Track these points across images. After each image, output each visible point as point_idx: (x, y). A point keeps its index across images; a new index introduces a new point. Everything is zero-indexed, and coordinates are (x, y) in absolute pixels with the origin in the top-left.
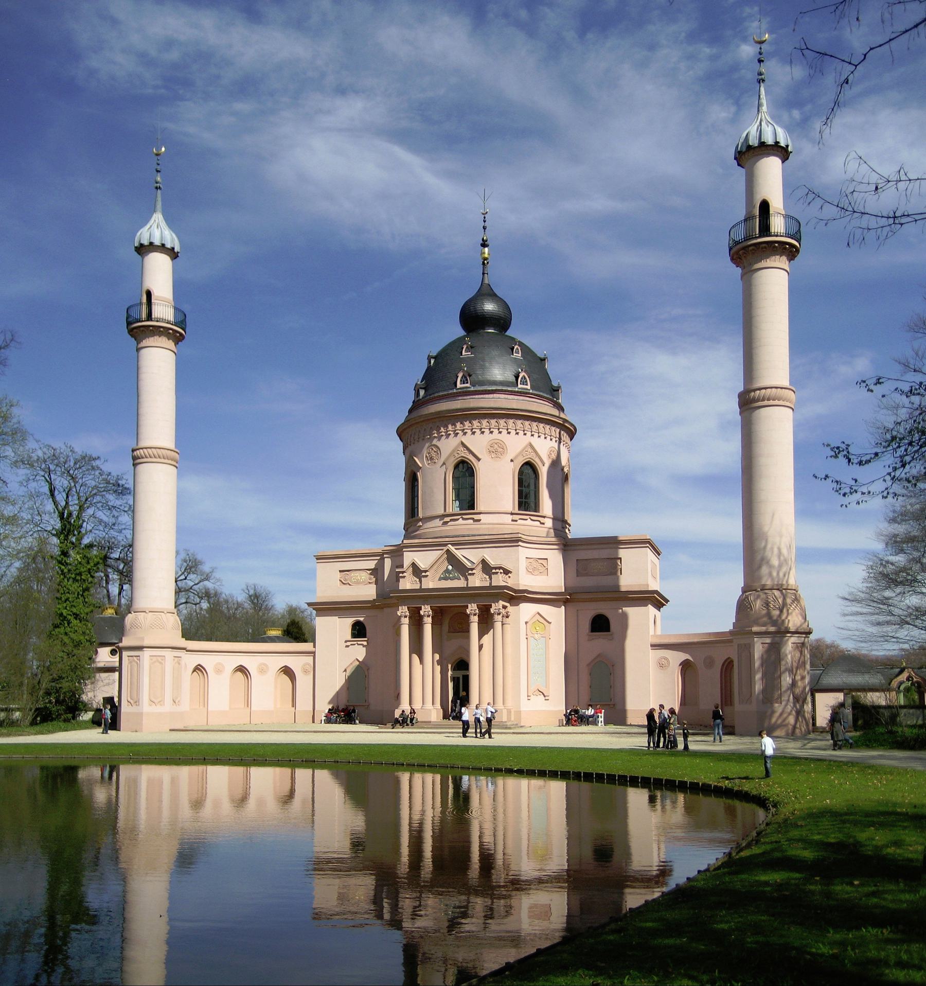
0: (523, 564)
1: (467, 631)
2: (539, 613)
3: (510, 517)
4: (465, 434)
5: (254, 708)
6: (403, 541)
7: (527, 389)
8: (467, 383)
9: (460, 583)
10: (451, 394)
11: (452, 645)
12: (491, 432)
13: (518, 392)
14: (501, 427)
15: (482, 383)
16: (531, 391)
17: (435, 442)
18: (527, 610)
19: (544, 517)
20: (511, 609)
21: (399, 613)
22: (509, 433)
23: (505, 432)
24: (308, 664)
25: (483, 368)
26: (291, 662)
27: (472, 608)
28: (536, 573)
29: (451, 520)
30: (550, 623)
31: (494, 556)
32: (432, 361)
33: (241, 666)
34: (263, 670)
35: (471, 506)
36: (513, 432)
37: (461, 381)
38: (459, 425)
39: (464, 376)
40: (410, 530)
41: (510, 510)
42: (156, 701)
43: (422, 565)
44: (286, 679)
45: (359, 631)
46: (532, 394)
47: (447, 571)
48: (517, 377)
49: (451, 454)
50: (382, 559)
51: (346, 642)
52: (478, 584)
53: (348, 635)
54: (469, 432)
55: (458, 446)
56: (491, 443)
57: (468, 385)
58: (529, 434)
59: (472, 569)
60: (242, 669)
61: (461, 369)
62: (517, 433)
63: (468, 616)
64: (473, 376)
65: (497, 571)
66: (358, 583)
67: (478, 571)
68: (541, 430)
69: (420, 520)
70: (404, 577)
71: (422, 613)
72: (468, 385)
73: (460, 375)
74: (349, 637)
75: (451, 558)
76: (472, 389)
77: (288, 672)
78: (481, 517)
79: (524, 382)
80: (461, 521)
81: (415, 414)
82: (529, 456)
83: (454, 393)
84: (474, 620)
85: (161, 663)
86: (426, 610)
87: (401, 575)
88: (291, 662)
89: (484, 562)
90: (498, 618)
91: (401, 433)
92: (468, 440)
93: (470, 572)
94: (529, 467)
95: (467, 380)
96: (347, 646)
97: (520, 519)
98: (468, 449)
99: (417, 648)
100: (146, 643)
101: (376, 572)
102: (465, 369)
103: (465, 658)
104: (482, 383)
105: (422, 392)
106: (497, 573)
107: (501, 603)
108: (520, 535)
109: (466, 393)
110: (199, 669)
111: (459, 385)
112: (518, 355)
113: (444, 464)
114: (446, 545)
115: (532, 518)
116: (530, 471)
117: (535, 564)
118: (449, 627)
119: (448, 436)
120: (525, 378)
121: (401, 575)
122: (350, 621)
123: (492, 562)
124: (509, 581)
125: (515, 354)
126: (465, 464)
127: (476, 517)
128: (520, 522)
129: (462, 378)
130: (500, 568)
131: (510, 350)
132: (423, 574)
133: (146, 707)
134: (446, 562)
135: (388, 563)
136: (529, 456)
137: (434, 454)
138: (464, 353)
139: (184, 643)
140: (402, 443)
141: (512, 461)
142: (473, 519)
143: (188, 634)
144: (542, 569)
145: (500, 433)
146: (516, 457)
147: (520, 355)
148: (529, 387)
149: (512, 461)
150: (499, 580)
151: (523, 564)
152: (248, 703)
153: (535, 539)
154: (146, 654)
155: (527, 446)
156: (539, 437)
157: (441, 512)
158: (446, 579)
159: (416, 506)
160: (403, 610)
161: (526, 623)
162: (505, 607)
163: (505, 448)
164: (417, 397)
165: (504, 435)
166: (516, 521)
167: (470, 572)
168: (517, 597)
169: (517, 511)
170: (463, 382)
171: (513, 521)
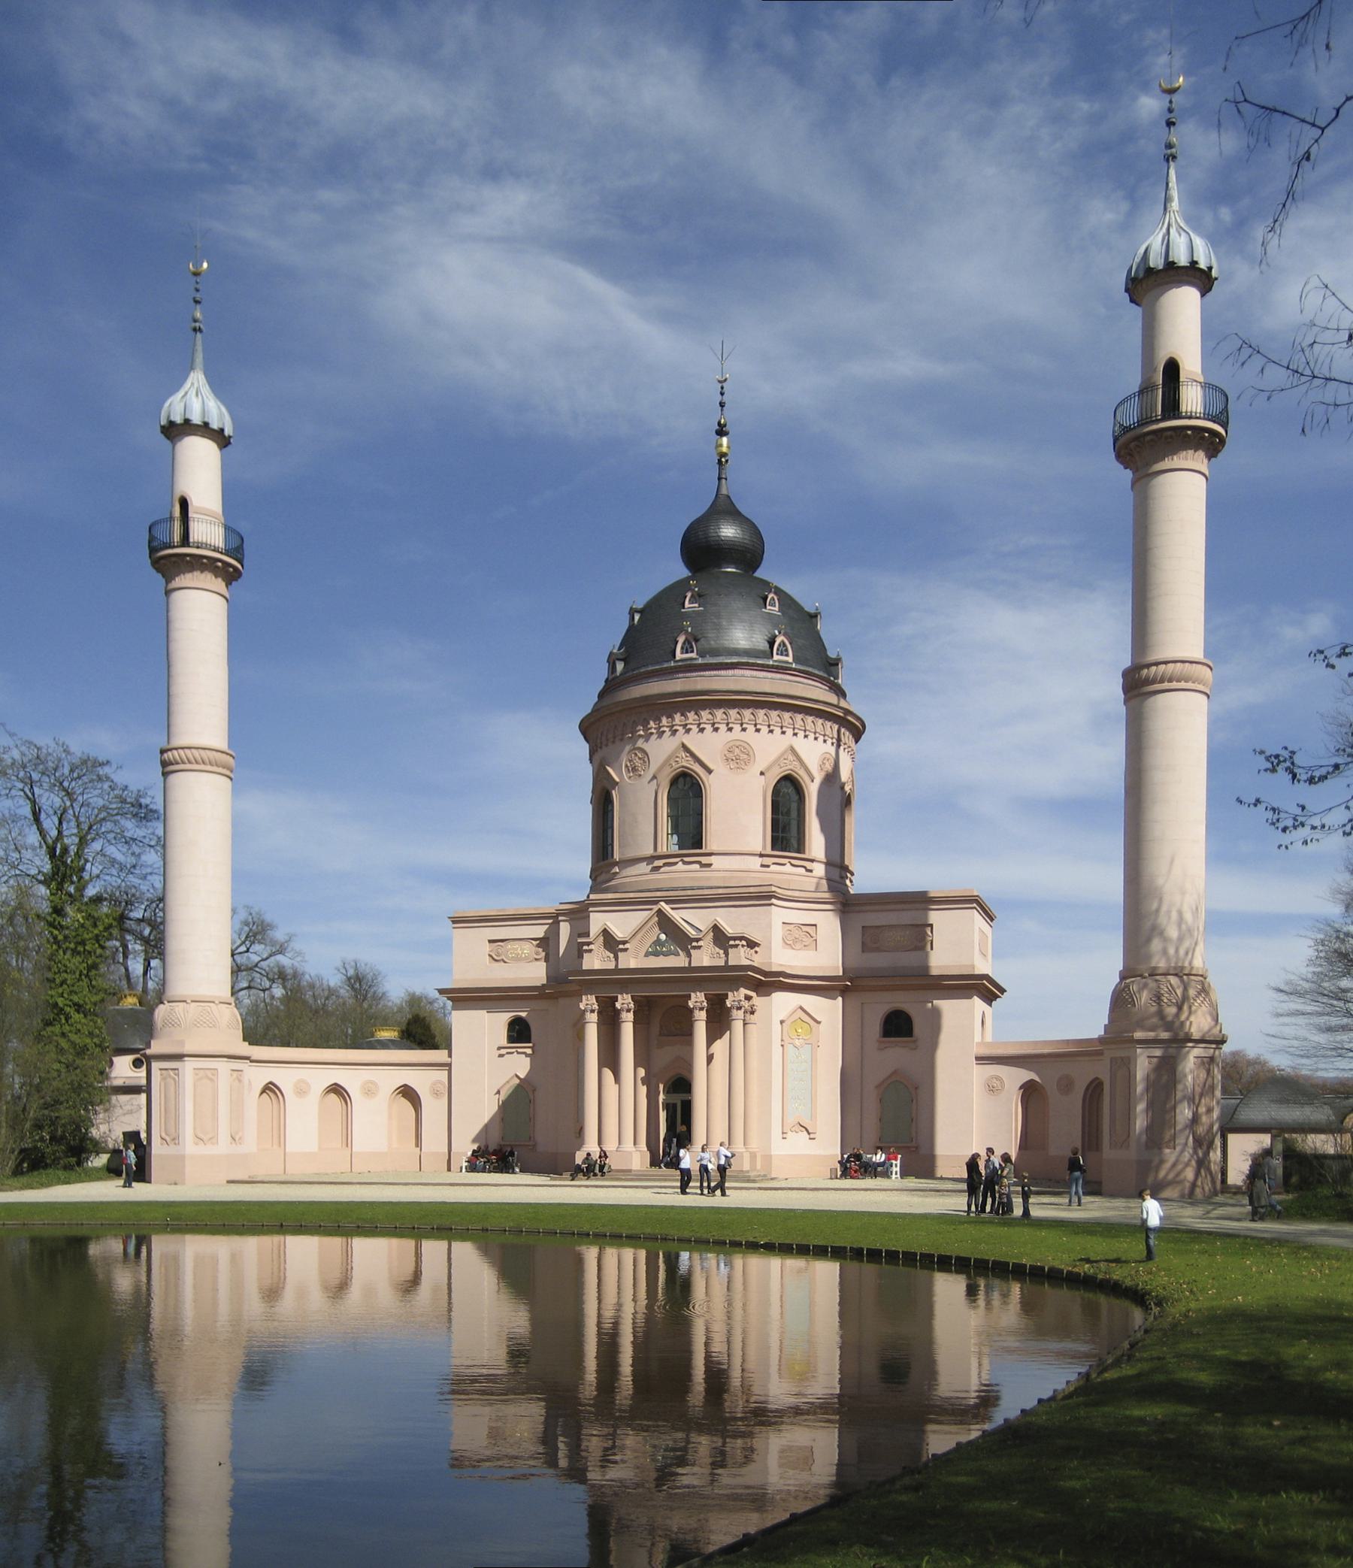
0: (777, 933)
1: (688, 1034)
2: (801, 1008)
3: (759, 861)
4: (688, 731)
6: (588, 897)
7: (787, 662)
8: (692, 652)
9: (679, 961)
10: (666, 669)
11: (664, 1056)
12: (730, 729)
13: (773, 667)
14: (746, 720)
15: (715, 653)
16: (794, 666)
17: (640, 743)
18: (783, 1003)
19: (812, 861)
20: (757, 1001)
21: (582, 1006)
22: (758, 730)
23: (751, 728)
24: (440, 1082)
25: (718, 628)
27: (697, 999)
28: (798, 946)
29: (665, 865)
30: (819, 1023)
31: (731, 920)
32: (637, 617)
33: (335, 1084)
34: (369, 1091)
35: (698, 843)
36: (764, 729)
37: (682, 648)
38: (678, 717)
39: (687, 641)
40: (600, 879)
41: (759, 849)
42: (205, 1139)
43: (619, 934)
44: (406, 1104)
45: (519, 1032)
46: (795, 670)
47: (658, 942)
48: (771, 643)
49: (667, 762)
50: (557, 923)
51: (499, 1048)
52: (706, 962)
53: (502, 1039)
54: (695, 728)
55: (676, 751)
56: (731, 744)
58: (790, 732)
59: (698, 940)
60: (336, 1089)
61: (682, 630)
62: (771, 731)
63: (691, 1011)
64: (702, 642)
65: (737, 942)
66: (518, 959)
67: (707, 943)
68: (810, 726)
69: (616, 864)
70: (590, 951)
71: (618, 1005)
72: (693, 655)
73: (681, 639)
74: (504, 1042)
75: (665, 923)
76: (700, 661)
77: (408, 1093)
79: (783, 651)
80: (680, 866)
81: (608, 701)
82: (790, 766)
83: (671, 668)
85: (211, 1080)
86: (624, 1001)
87: (585, 948)
89: (716, 929)
90: (738, 1015)
91: (587, 728)
92: (693, 740)
93: (694, 944)
94: (789, 784)
95: (692, 647)
96: (501, 1056)
97: (774, 864)
99: (610, 1058)
101: (546, 943)
102: (690, 629)
104: (715, 653)
105: (620, 666)
106: (736, 946)
107: (743, 991)
108: (774, 889)
109: (689, 668)
110: (270, 1089)
111: (679, 655)
112: (774, 609)
113: (654, 777)
114: (656, 903)
115: (793, 862)
116: (791, 790)
117: (797, 933)
118: (661, 1027)
119: (661, 734)
120: (784, 645)
121: (585, 948)
122: (503, 1018)
123: (729, 930)
124: (756, 958)
125: (768, 607)
126: (688, 779)
127: (704, 860)
128: (773, 868)
129: (684, 643)
130: (741, 938)
131: (762, 601)
132: (621, 946)
133: (190, 1146)
134: (657, 929)
135: (565, 929)
136: (790, 767)
137: (638, 763)
138: (687, 604)
139: (245, 1049)
140: (587, 746)
141: (762, 773)
142: (699, 863)
143: (254, 1035)
144: (808, 940)
145: (744, 730)
146: (769, 768)
147: (777, 609)
148: (790, 659)
149: (762, 773)
150: (740, 956)
151: (777, 933)
152: (347, 1140)
153: (797, 894)
154: (189, 1066)
155: (785, 752)
156: (806, 736)
157: (649, 851)
158: (656, 954)
159: (610, 842)
160: (589, 1002)
161: (782, 1022)
162: (748, 998)
163: (751, 753)
164: (612, 673)
166: (768, 866)
167: (694, 944)
168: (768, 983)
169: (769, 851)
170: (685, 651)
171: (762, 866)
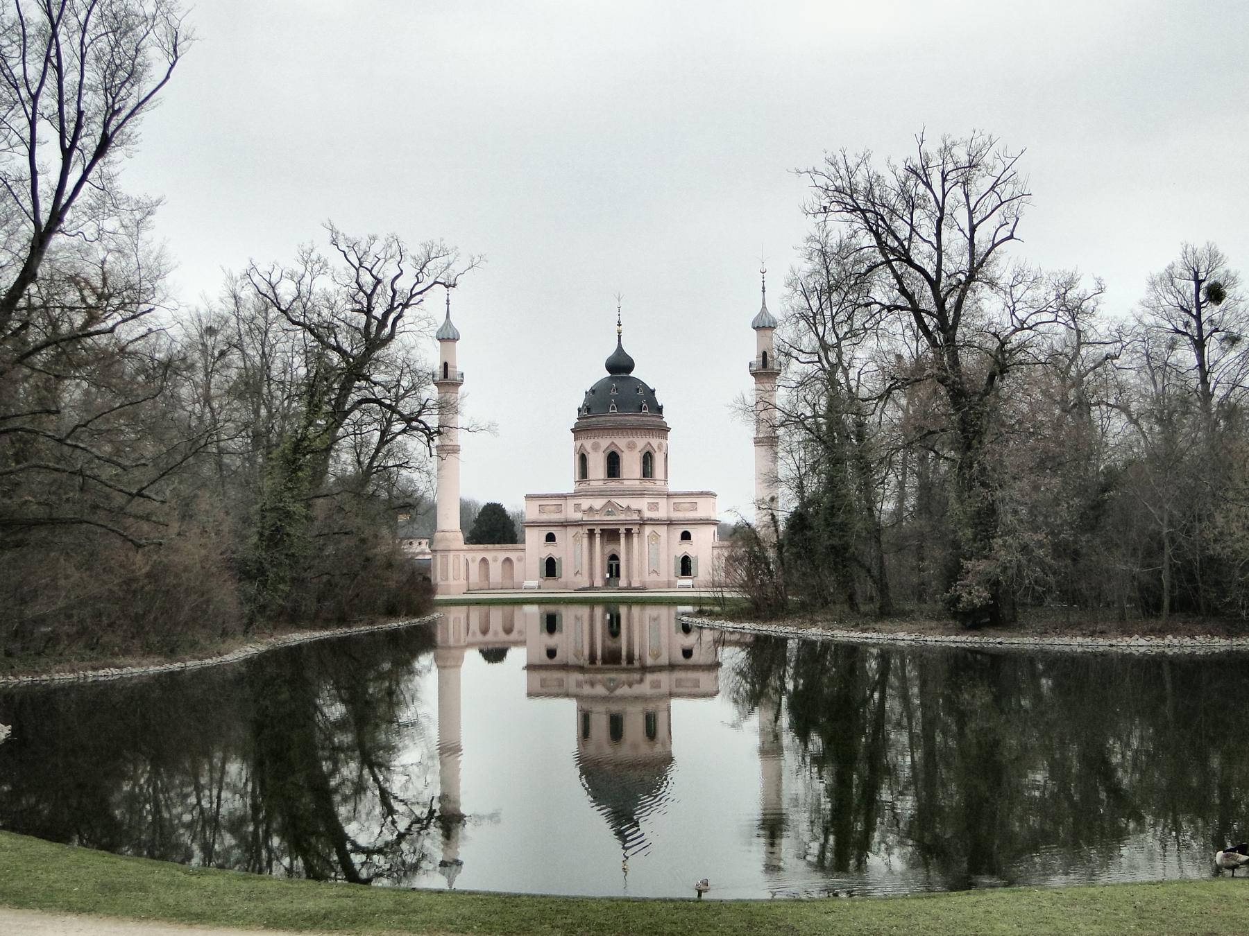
1: (619, 540)
11: (610, 549)
26: (513, 556)
45: (550, 538)
63: (619, 535)
86: (597, 531)
100: (453, 547)
110: (484, 560)
122: (545, 531)
123: (634, 507)
133: (451, 581)
139: (465, 547)
143: (468, 541)
151: (647, 506)
154: (451, 555)
157: (602, 477)
168: (643, 523)
170: (613, 408)
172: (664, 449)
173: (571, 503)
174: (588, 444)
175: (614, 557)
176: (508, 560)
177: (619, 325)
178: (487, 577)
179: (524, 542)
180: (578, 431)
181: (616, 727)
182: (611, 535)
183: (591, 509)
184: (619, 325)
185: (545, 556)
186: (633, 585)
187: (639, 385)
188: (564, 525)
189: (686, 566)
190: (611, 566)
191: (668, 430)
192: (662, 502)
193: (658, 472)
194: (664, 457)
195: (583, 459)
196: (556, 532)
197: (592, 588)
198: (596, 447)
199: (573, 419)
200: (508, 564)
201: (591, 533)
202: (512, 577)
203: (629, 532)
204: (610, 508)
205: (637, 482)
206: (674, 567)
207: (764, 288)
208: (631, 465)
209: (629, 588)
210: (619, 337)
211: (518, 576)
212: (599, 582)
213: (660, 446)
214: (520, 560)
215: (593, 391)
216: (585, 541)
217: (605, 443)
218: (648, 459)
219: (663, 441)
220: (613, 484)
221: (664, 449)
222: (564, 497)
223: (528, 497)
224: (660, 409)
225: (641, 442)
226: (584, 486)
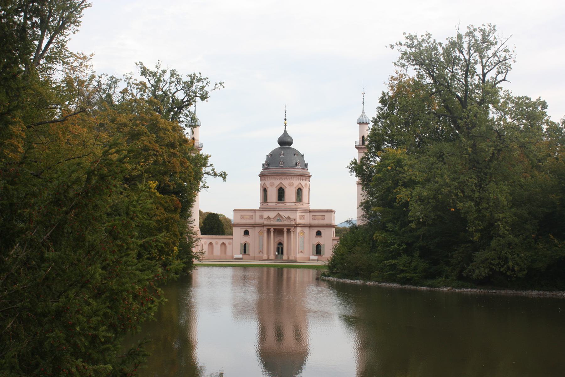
5: (214, 254)
11: (278, 239)
26: (224, 241)
27: (285, 229)
31: (291, 215)
34: (217, 243)
40: (265, 205)
41: (294, 201)
45: (246, 233)
48: (296, 164)
57: (283, 166)
78: (287, 204)
82: (300, 186)
84: (285, 233)
88: (224, 241)
98: (283, 184)
103: (282, 242)
117: (301, 217)
122: (244, 229)
123: (291, 217)
127: (285, 203)
144: (303, 218)
146: (296, 187)
151: (298, 217)
155: (298, 185)
157: (275, 201)
158: (278, 221)
165: (292, 181)
168: (296, 226)
169: (296, 202)
172: (308, 186)
173: (258, 214)
174: (268, 183)
175: (280, 244)
176: (223, 244)
177: (285, 120)
178: (212, 253)
179: (231, 234)
180: (262, 176)
181: (279, 335)
182: (279, 232)
183: (269, 218)
184: (285, 120)
185: (243, 242)
186: (291, 259)
187: (296, 153)
188: (254, 226)
189: (318, 249)
190: (278, 248)
191: (310, 176)
192: (307, 215)
193: (305, 199)
194: (307, 190)
195: (265, 191)
196: (250, 230)
197: (268, 260)
198: (272, 185)
199: (260, 169)
200: (223, 246)
201: (269, 231)
202: (225, 253)
203: (289, 231)
204: (279, 216)
205: (294, 204)
206: (312, 249)
207: (363, 102)
208: (290, 194)
209: (288, 260)
210: (285, 126)
211: (229, 253)
212: (272, 257)
213: (306, 184)
214: (230, 244)
215: (271, 155)
216: (265, 234)
217: (277, 182)
218: (299, 191)
219: (307, 182)
220: (281, 205)
221: (308, 186)
222: (254, 211)
223: (235, 211)
224: (306, 165)
225: (296, 183)
226: (265, 206)
